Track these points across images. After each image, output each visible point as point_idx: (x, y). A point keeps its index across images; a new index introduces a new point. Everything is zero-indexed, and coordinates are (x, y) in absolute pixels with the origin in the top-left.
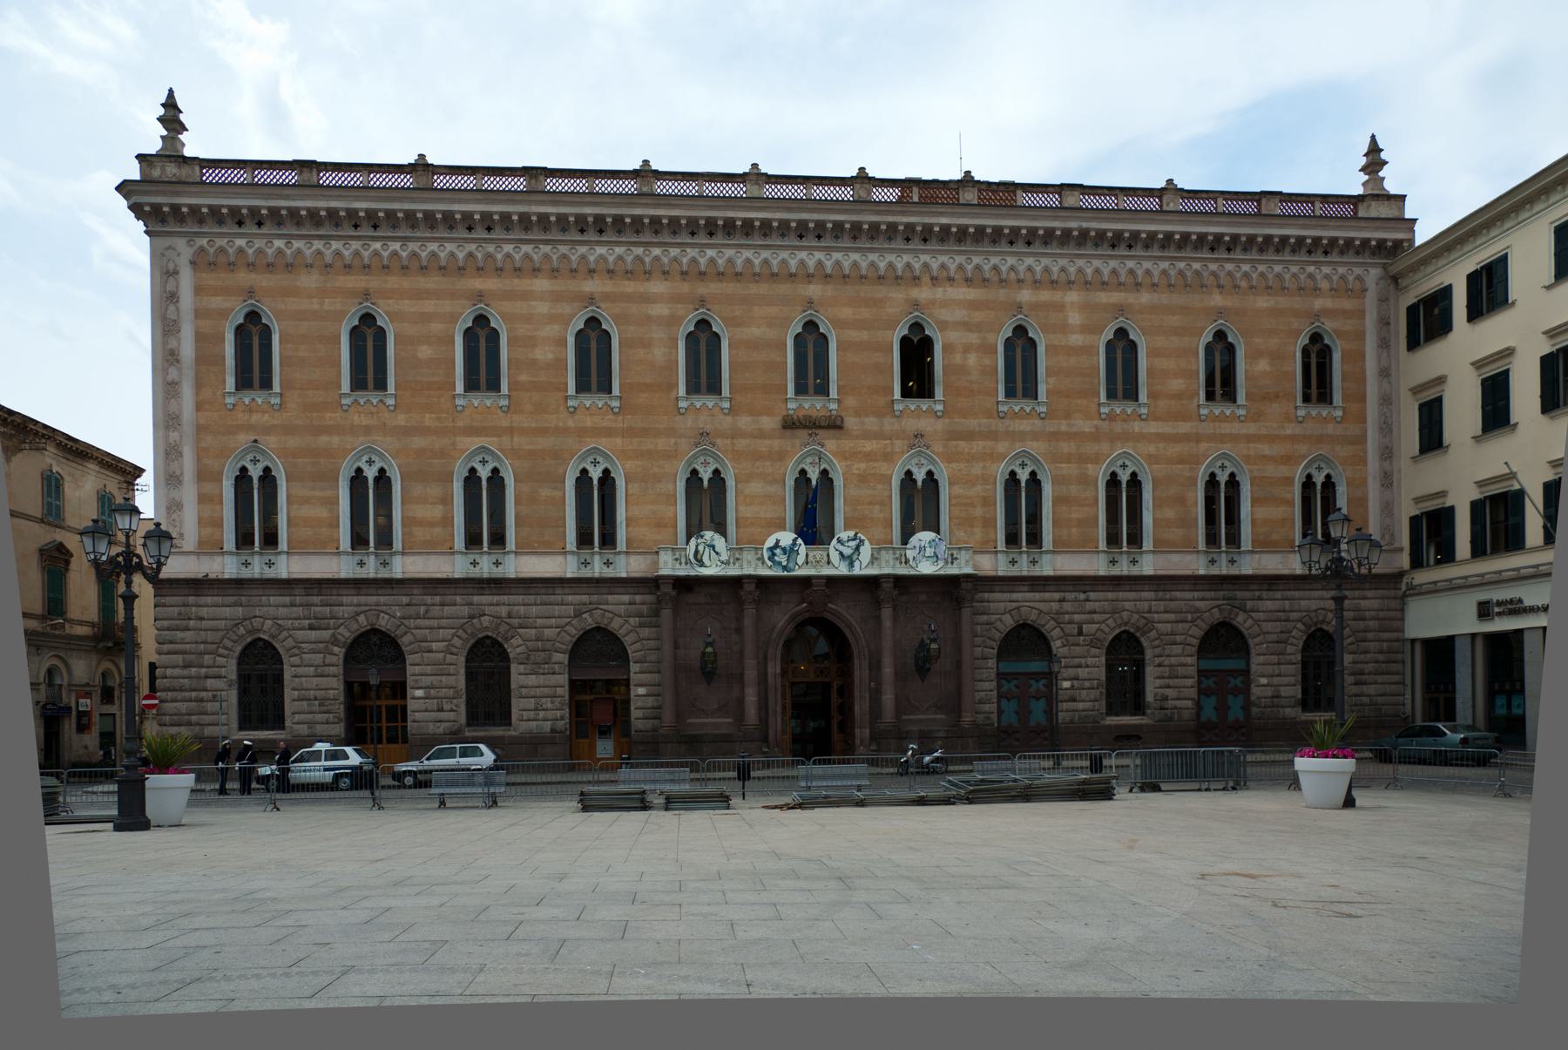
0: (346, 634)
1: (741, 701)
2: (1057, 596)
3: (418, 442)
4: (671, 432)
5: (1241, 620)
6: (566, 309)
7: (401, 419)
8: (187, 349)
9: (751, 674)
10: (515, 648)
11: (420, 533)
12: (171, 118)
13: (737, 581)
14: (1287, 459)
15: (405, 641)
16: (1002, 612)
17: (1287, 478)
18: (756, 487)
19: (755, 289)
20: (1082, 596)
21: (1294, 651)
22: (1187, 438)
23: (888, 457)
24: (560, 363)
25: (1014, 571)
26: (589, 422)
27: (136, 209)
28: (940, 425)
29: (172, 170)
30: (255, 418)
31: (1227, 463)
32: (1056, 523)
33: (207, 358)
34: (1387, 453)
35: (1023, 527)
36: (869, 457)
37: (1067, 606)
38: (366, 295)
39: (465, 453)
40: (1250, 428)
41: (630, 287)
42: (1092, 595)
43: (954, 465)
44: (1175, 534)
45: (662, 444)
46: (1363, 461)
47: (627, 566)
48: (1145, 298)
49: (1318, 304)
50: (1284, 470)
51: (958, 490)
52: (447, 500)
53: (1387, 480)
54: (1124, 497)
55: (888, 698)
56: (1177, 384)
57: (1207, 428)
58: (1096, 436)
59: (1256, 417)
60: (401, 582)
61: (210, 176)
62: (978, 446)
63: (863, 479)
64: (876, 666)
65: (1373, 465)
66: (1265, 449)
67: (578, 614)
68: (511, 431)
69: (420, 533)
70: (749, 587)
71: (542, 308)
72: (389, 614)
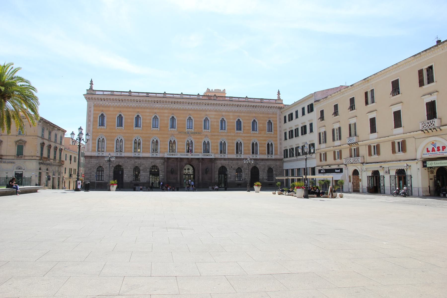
0: (114, 166)
1: (177, 177)
3: (127, 135)
5: (257, 166)
6: (152, 114)
7: (125, 131)
8: (92, 119)
9: (179, 173)
10: (141, 168)
11: (127, 149)
12: (91, 83)
13: (177, 158)
14: (265, 140)
15: (124, 167)
16: (219, 164)
19: (181, 112)
21: (266, 171)
23: (202, 139)
24: (150, 123)
25: (221, 157)
27: (86, 98)
29: (92, 92)
30: (102, 131)
32: (228, 150)
33: (95, 121)
34: (281, 140)
35: (222, 151)
36: (198, 138)
38: (120, 112)
39: (136, 137)
40: (259, 135)
41: (162, 111)
44: (247, 152)
46: (277, 141)
47: (159, 155)
48: (243, 114)
49: (270, 116)
50: (264, 142)
52: (131, 144)
53: (281, 144)
54: (238, 146)
55: (200, 178)
56: (247, 128)
58: (234, 136)
59: (260, 133)
60: (123, 157)
61: (97, 93)
62: (216, 137)
63: (197, 142)
64: (199, 172)
65: (278, 142)
66: (261, 138)
67: (151, 163)
68: (142, 133)
69: (127, 149)
70: (179, 159)
71: (148, 114)
72: (121, 162)
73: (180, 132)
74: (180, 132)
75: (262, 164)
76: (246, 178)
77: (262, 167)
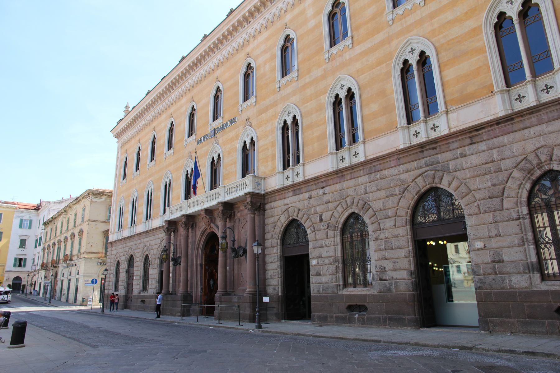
2: (307, 195)
16: (277, 216)
17: (474, 30)
20: (321, 192)
22: (382, 44)
31: (415, 46)
35: (290, 154)
37: (313, 202)
42: (327, 189)
50: (471, 24)
57: (397, 27)
75: (475, 160)
76: (388, 265)
77: (474, 184)
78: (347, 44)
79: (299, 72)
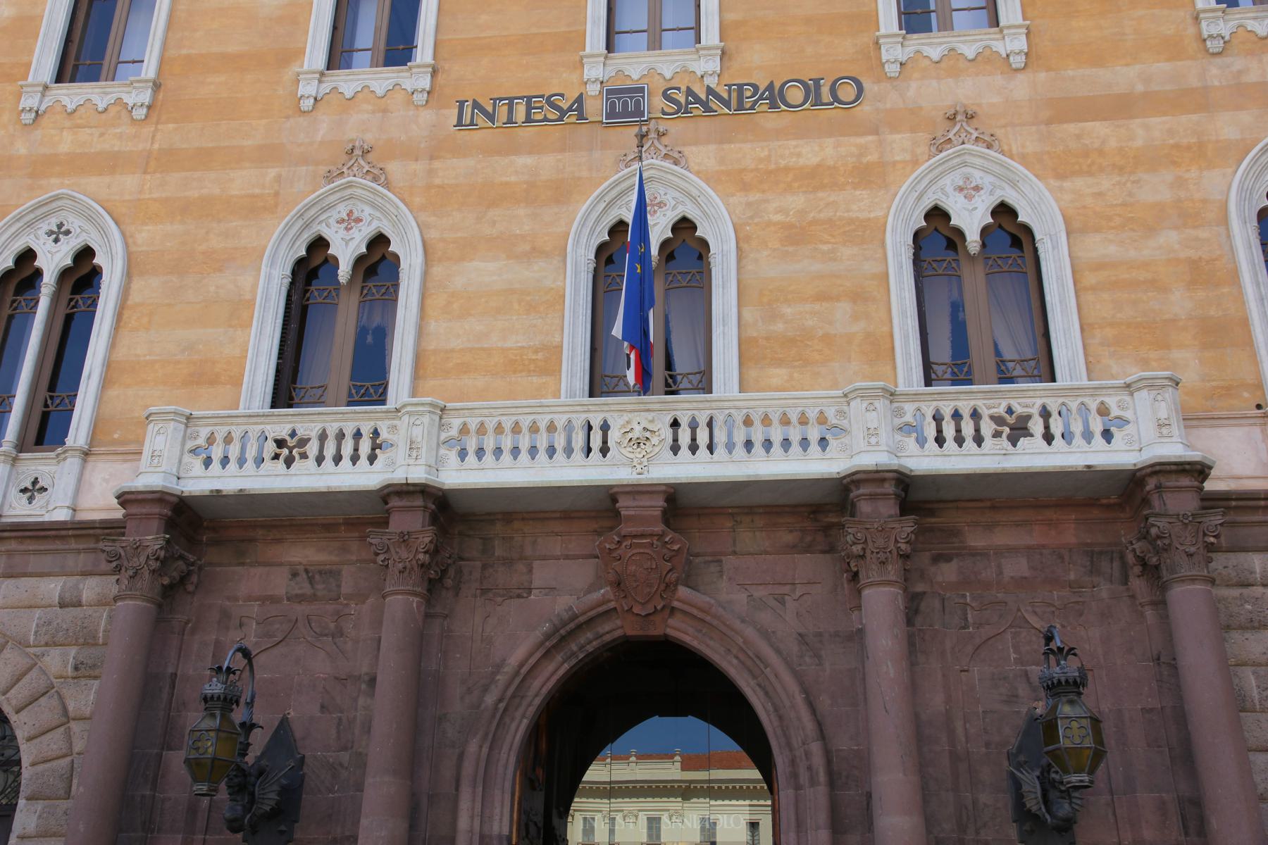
4: (268, 154)
18: (484, 272)
23: (870, 175)
26: (66, 143)
28: (1021, 87)
36: (814, 178)
43: (1079, 183)
45: (241, 181)
51: (1098, 247)
62: (1148, 130)
63: (797, 235)
73: (474, 113)
74: (474, 113)
78: (408, 85)
79: (441, 78)
